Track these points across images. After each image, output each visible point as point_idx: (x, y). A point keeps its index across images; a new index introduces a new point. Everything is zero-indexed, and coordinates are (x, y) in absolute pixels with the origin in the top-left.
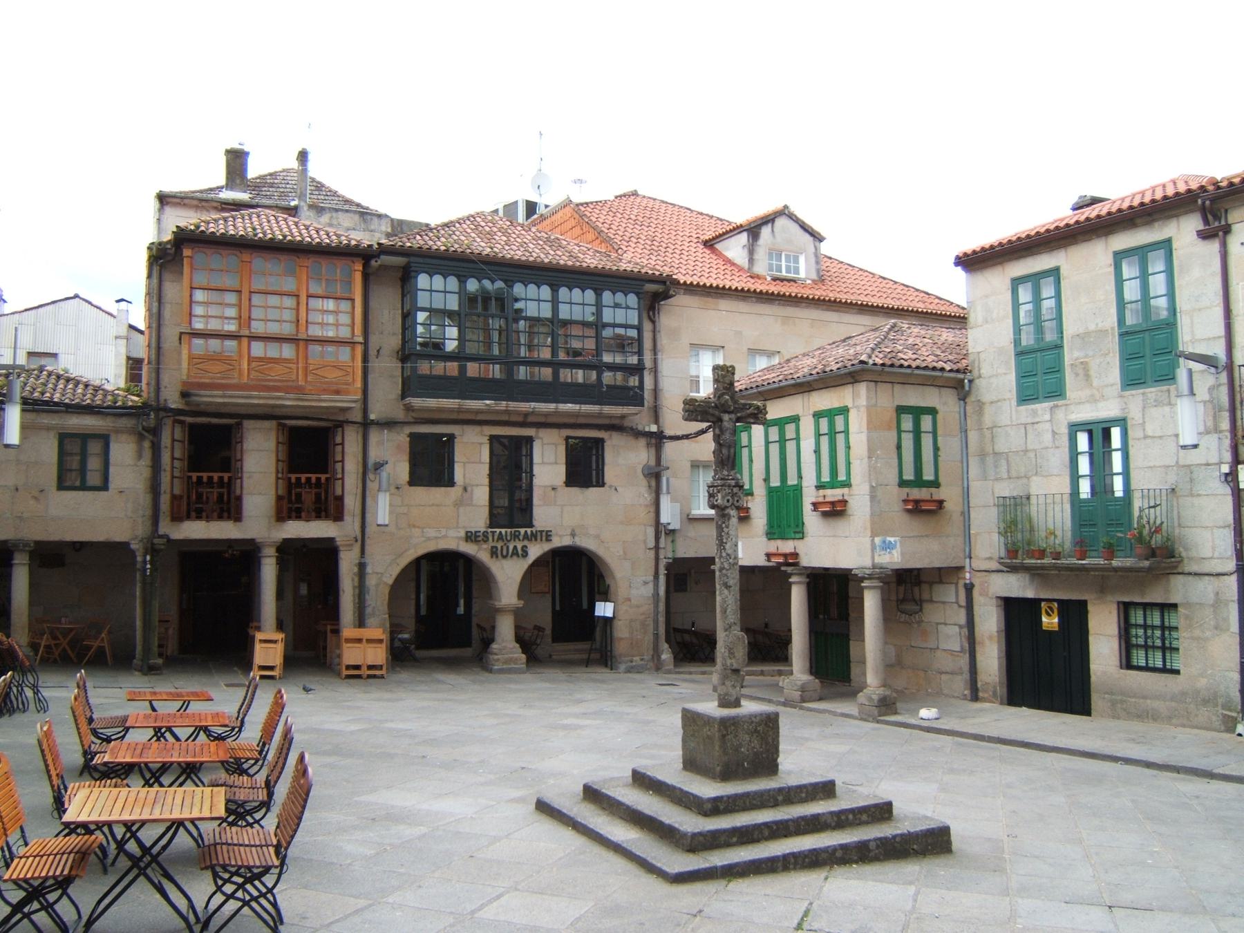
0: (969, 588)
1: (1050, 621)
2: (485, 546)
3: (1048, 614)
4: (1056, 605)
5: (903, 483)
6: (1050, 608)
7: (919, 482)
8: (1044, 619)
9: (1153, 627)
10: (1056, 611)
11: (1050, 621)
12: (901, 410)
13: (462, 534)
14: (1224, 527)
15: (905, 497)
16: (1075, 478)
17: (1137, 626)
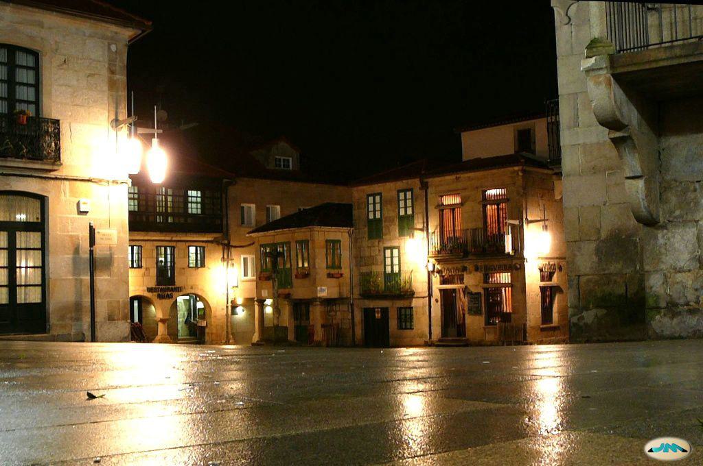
0: (352, 305)
1: (378, 315)
2: (154, 294)
5: (327, 268)
7: (333, 267)
11: (378, 315)
12: (327, 241)
13: (146, 289)
15: (328, 272)
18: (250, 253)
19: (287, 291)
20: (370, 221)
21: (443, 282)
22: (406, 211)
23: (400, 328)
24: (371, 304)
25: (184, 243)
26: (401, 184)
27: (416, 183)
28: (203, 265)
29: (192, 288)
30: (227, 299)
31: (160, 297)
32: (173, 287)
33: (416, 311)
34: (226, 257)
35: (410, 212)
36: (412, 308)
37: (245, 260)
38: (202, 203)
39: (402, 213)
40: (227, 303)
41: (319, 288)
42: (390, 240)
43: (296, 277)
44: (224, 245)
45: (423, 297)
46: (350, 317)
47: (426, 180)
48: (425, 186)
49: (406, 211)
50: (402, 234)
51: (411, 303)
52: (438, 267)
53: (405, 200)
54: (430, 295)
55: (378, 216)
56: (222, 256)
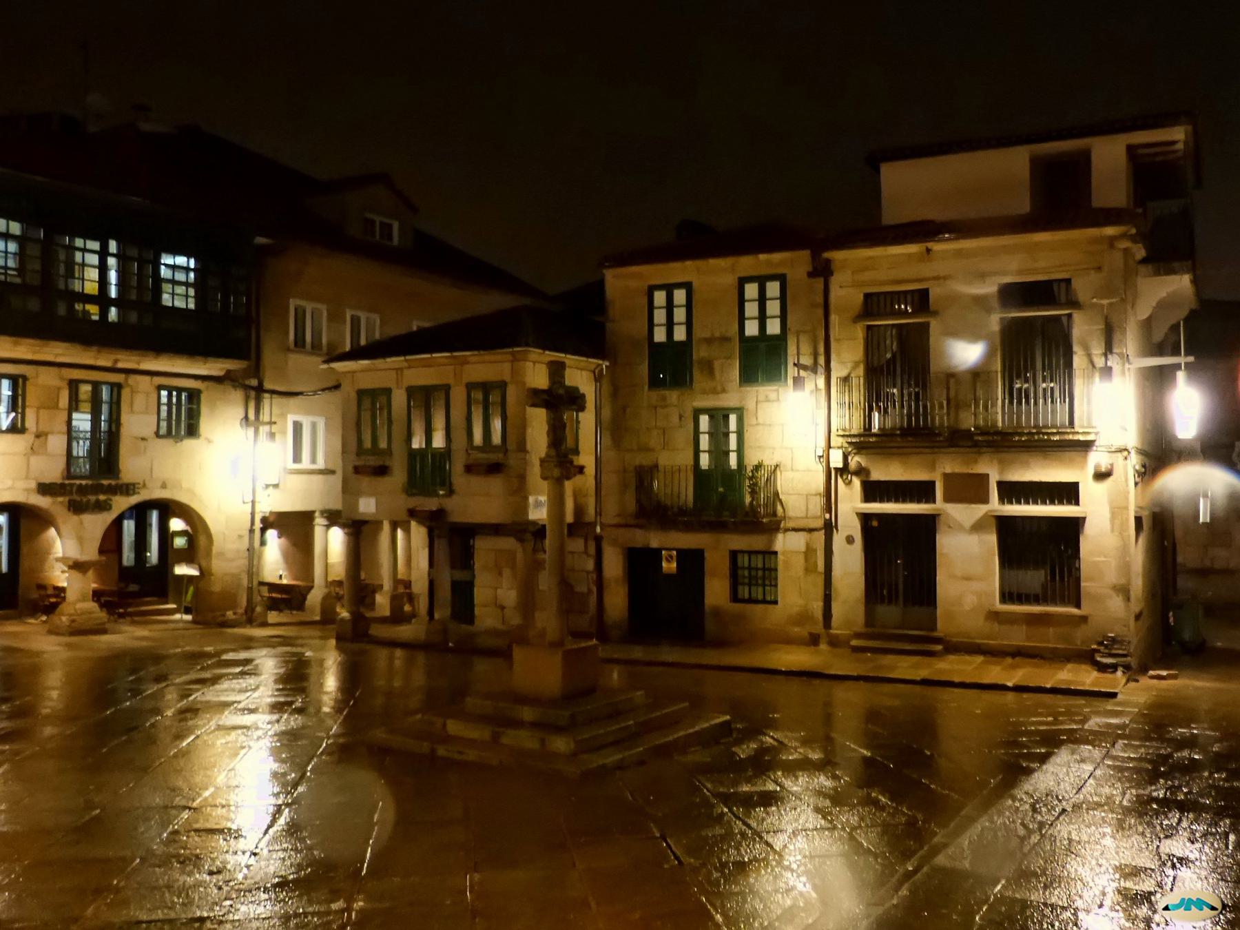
0: (598, 540)
1: (669, 566)
3: (667, 560)
4: (675, 553)
6: (671, 557)
8: (664, 564)
9: (757, 569)
10: (675, 558)
14: (816, 495)
16: (697, 452)
17: (743, 568)
18: (308, 412)
19: (431, 504)
20: (654, 348)
21: (872, 491)
22: (763, 326)
23: (735, 598)
24: (655, 540)
25: (147, 378)
26: (748, 264)
27: (796, 263)
28: (192, 431)
29: (164, 486)
30: (253, 514)
31: (77, 508)
32: (113, 483)
33: (786, 563)
34: (252, 416)
35: (774, 327)
36: (776, 553)
37: (298, 427)
38: (199, 285)
39: (752, 329)
40: (253, 523)
41: (531, 499)
42: (714, 392)
43: (469, 469)
44: (247, 388)
45: (811, 530)
46: (590, 565)
47: (826, 255)
48: (823, 271)
49: (763, 326)
50: (748, 377)
51: (771, 542)
52: (854, 461)
53: (762, 300)
54: (829, 528)
55: (680, 334)
56: (242, 415)
